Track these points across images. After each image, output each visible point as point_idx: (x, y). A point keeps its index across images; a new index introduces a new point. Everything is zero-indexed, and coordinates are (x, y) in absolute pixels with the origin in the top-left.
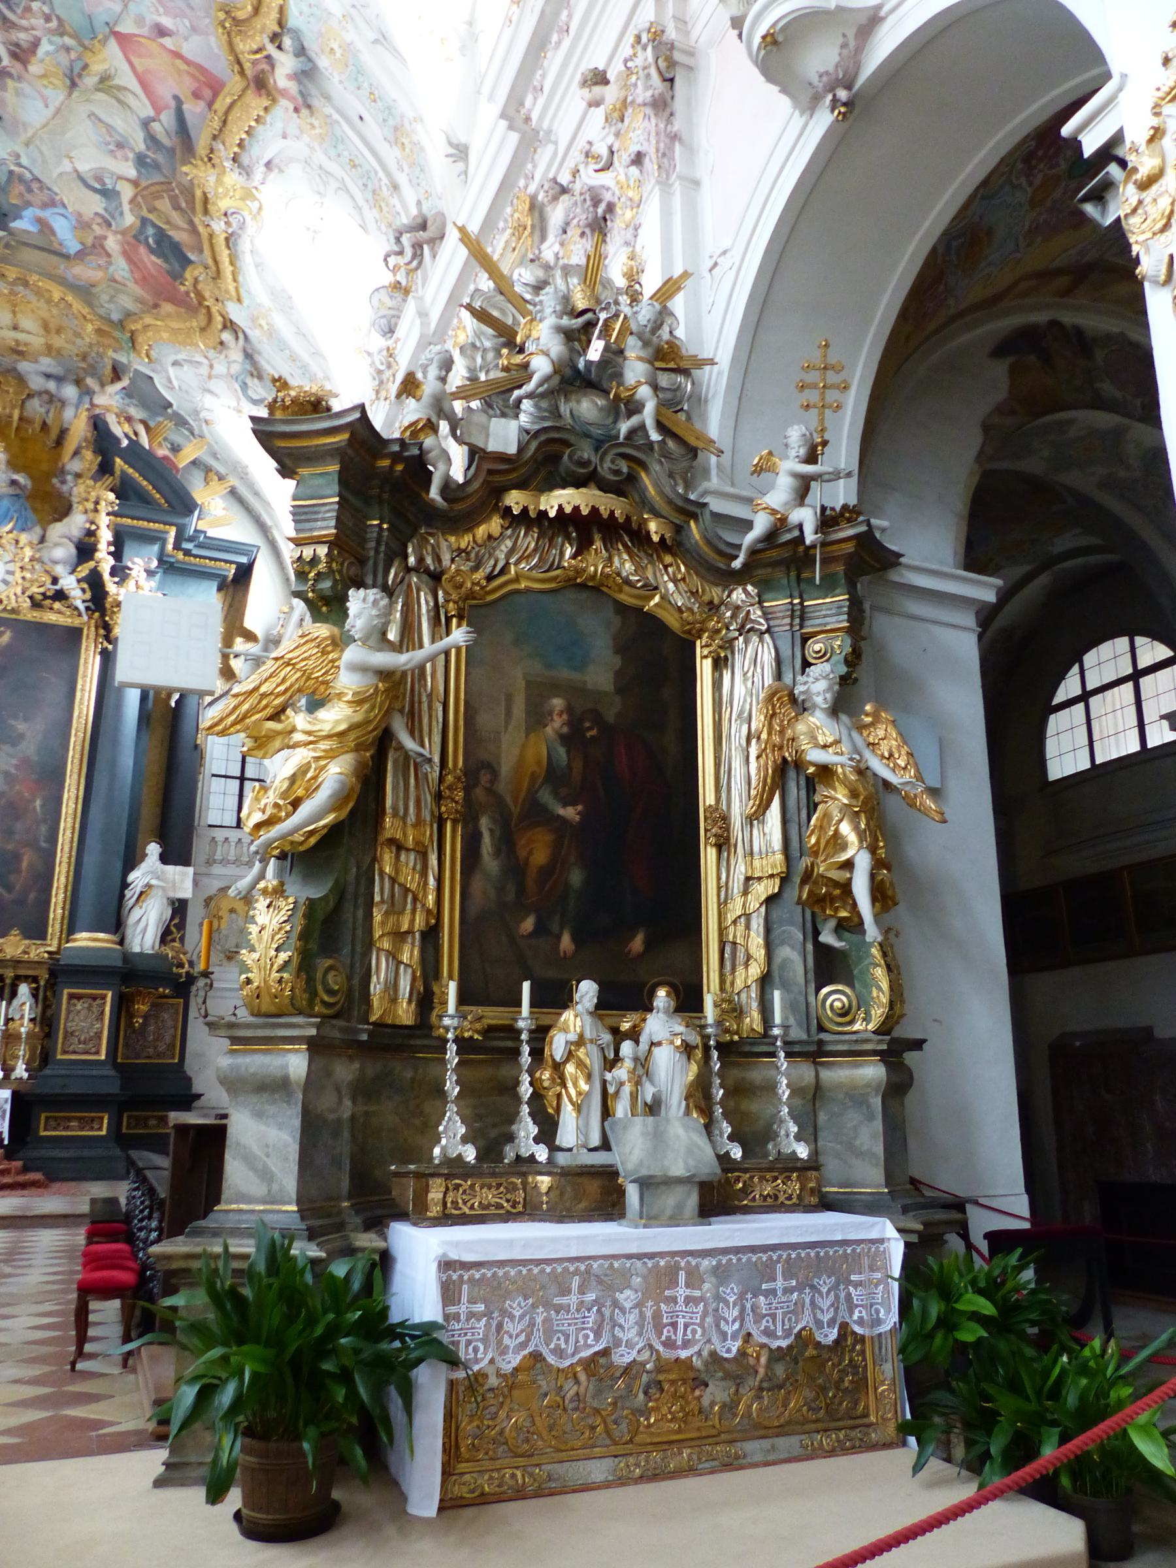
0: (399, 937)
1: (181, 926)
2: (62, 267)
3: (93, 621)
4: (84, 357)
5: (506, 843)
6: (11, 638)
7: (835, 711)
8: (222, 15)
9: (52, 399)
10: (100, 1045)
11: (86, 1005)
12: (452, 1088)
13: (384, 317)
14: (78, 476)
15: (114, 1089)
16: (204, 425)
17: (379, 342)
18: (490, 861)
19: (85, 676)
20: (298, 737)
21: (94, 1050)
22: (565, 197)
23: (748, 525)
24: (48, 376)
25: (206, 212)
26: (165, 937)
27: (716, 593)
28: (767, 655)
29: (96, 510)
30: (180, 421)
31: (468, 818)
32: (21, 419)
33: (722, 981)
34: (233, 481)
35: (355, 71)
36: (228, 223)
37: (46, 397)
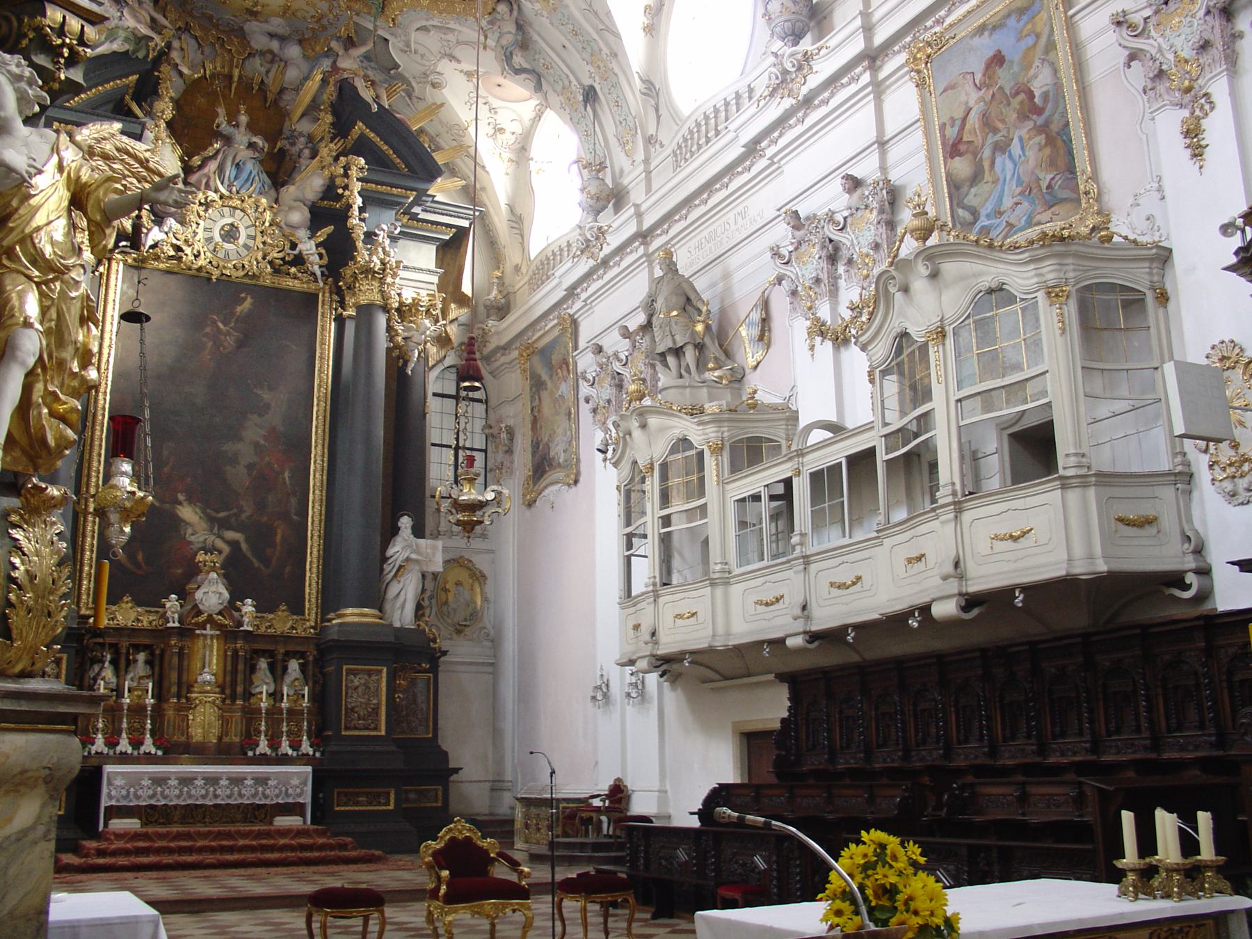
1: (423, 599)
3: (327, 287)
6: (252, 304)
9: (273, 58)
10: (378, 720)
11: (362, 681)
13: (789, 20)
16: (429, 87)
19: (323, 343)
21: (373, 726)
24: (272, 36)
29: (346, 175)
32: (240, 77)
37: (269, 57)
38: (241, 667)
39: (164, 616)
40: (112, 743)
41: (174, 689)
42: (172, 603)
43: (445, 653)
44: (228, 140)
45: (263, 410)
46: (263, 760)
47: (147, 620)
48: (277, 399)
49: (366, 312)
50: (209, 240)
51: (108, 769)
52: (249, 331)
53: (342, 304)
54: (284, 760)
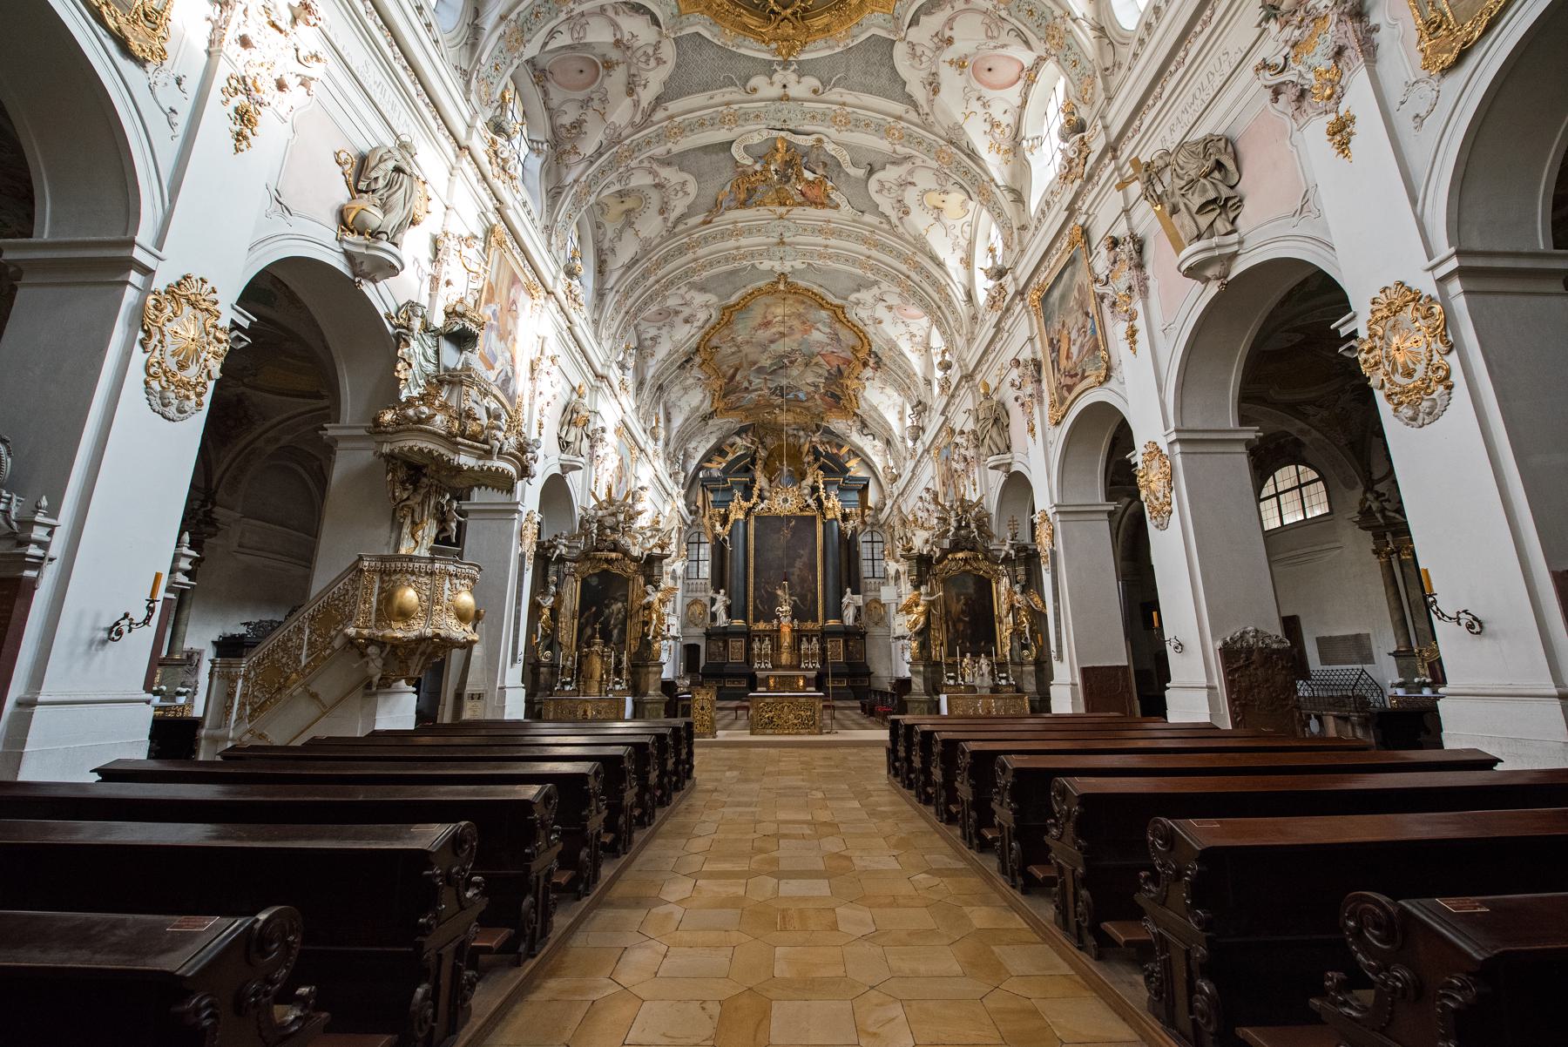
0: (936, 646)
5: (954, 626)
7: (1022, 593)
14: (809, 463)
15: (847, 671)
26: (856, 619)
28: (1008, 581)
30: (838, 436)
31: (947, 622)
42: (775, 622)
44: (782, 470)
46: (803, 670)
48: (804, 552)
49: (831, 520)
52: (794, 531)
54: (810, 670)
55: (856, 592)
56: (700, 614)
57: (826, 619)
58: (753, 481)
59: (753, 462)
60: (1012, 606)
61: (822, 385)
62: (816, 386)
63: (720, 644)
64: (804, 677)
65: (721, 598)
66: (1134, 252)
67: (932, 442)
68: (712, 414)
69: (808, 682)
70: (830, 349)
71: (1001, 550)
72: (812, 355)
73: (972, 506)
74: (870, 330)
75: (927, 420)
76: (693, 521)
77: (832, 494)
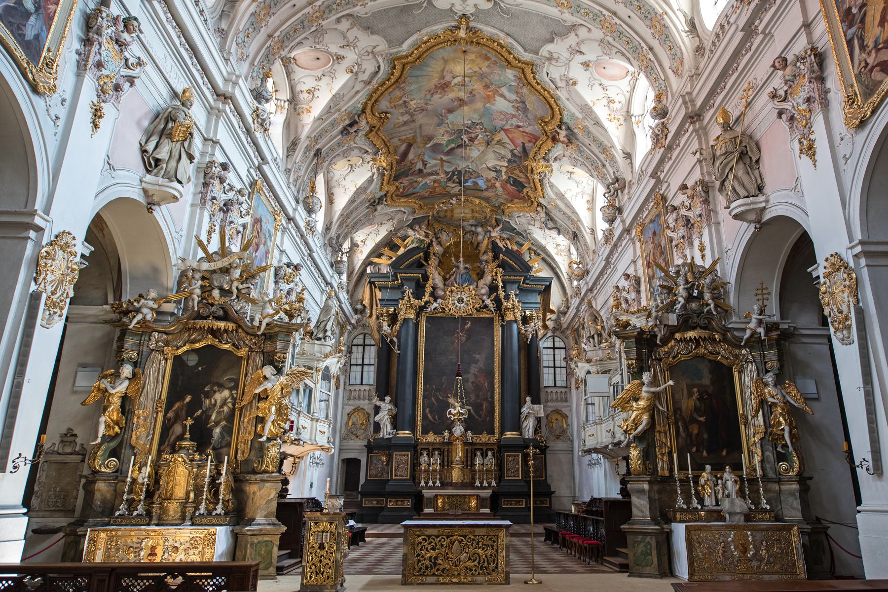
1: (540, 427)
2: (480, 194)
4: (485, 218)
5: (686, 428)
7: (775, 385)
8: (540, 121)
12: (679, 492)
14: (486, 261)
17: (606, 226)
18: (683, 434)
20: (634, 409)
22: (676, 211)
23: (744, 330)
25: (532, 173)
26: (536, 431)
27: (737, 351)
30: (519, 234)
31: (676, 423)
33: (750, 462)
34: (543, 255)
35: (586, 130)
36: (541, 176)
38: (469, 455)
39: (444, 438)
40: (427, 483)
41: (446, 464)
42: (446, 433)
43: (548, 447)
44: (458, 267)
45: (476, 362)
46: (478, 488)
47: (438, 439)
48: (480, 357)
50: (454, 304)
51: (423, 491)
52: (470, 334)
53: (503, 320)
55: (536, 401)
56: (362, 424)
57: (503, 431)
58: (426, 278)
59: (427, 258)
60: (762, 403)
61: (504, 170)
62: (498, 171)
63: (384, 459)
64: (478, 496)
65: (386, 406)
66: (815, 64)
67: (635, 218)
68: (380, 199)
69: (481, 502)
70: (515, 122)
71: (744, 330)
72: (495, 131)
73: (703, 273)
74: (562, 94)
75: (626, 197)
76: (358, 321)
77: (512, 296)
